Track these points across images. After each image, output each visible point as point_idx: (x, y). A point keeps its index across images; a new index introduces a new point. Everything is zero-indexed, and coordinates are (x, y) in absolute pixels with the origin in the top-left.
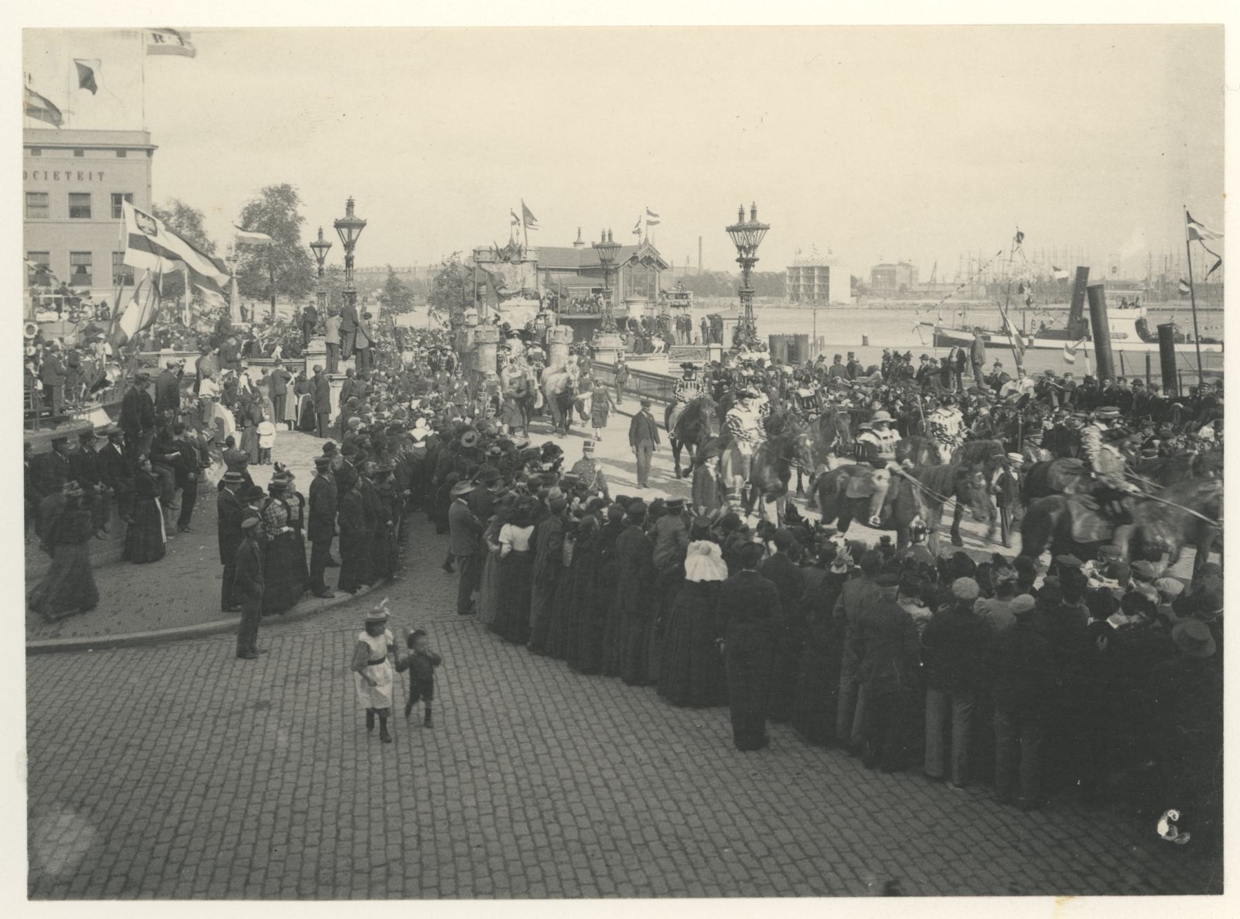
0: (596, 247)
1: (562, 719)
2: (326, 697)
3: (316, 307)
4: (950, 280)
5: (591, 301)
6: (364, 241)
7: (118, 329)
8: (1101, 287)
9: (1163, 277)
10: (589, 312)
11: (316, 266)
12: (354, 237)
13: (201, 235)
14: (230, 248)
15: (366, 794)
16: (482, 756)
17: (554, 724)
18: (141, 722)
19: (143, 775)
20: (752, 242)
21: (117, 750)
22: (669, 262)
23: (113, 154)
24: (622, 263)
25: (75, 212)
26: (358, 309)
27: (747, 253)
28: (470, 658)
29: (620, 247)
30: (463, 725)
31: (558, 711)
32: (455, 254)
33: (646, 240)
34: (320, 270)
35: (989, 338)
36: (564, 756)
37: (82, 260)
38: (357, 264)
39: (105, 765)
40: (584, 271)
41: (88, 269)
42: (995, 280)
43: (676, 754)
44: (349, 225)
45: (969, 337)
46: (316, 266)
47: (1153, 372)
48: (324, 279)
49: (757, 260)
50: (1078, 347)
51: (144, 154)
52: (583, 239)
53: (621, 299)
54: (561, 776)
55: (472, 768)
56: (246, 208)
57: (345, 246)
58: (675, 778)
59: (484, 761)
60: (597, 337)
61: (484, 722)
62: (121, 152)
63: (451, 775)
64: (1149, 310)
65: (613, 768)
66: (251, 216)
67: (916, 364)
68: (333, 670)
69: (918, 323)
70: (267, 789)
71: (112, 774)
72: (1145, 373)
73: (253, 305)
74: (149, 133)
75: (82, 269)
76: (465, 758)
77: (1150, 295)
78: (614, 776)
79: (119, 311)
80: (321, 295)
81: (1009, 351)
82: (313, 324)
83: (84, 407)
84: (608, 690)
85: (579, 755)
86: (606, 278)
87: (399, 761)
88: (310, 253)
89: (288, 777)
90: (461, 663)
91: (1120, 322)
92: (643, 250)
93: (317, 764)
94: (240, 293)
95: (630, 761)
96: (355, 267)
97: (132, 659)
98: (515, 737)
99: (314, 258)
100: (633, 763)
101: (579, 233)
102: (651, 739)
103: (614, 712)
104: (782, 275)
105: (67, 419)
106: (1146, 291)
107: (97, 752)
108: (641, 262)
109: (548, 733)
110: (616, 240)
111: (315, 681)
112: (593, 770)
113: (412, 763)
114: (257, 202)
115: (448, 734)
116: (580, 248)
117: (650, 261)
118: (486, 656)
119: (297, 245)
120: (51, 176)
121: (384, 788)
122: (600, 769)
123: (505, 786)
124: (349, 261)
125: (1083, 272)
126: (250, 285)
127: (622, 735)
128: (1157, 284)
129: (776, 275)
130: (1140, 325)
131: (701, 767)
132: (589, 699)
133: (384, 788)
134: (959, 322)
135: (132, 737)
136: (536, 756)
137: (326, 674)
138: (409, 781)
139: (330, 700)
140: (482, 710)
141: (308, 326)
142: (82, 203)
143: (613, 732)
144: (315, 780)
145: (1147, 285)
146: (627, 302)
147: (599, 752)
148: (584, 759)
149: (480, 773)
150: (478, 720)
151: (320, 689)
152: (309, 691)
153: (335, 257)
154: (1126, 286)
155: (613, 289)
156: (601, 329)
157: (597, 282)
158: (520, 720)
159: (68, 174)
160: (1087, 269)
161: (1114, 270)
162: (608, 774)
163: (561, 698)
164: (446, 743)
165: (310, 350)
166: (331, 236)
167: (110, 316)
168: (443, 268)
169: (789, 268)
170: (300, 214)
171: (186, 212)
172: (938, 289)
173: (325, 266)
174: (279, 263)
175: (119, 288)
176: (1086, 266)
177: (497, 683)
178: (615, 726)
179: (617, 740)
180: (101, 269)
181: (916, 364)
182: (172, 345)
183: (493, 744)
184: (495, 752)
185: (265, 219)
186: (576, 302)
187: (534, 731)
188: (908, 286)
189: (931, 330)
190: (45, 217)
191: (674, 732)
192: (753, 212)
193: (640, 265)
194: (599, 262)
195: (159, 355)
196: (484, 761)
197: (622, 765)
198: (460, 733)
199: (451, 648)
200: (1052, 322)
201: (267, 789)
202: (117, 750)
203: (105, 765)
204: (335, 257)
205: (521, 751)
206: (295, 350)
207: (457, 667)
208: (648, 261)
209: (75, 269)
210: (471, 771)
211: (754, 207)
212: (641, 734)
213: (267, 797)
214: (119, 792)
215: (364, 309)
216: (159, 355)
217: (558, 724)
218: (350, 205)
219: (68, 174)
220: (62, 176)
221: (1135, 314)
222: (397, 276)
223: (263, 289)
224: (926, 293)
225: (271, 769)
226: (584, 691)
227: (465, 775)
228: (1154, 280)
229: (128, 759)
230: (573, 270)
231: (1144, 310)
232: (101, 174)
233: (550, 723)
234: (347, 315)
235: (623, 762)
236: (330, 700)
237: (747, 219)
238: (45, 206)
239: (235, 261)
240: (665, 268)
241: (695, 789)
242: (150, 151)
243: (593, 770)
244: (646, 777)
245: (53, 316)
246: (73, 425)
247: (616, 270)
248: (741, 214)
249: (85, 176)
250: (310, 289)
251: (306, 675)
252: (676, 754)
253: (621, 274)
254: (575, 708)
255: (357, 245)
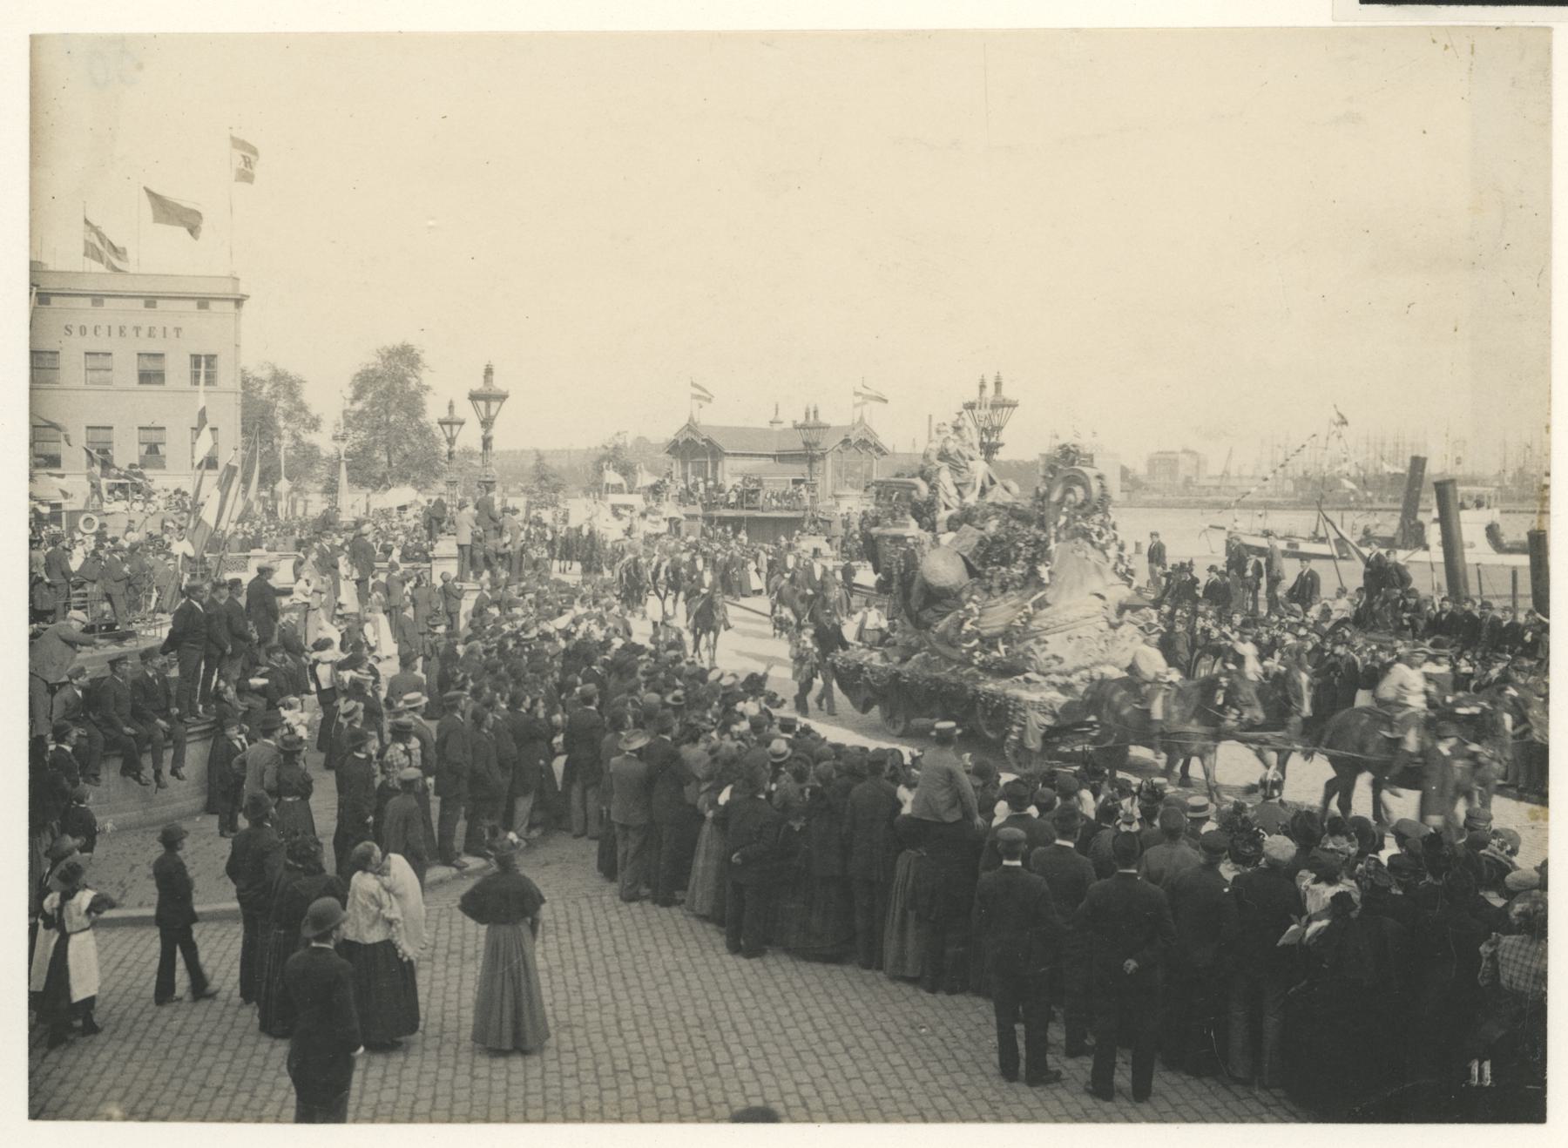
0: (796, 427)
1: (751, 1022)
2: (454, 988)
3: (445, 499)
4: (1248, 471)
5: (792, 495)
6: (505, 417)
7: (199, 522)
8: (1452, 481)
9: (1521, 470)
10: (788, 509)
11: (445, 448)
12: (493, 412)
13: (302, 408)
14: (338, 425)
15: (503, 1110)
16: (648, 1065)
17: (739, 1026)
18: (222, 1016)
19: (224, 1082)
20: (996, 423)
21: (194, 1050)
22: (890, 448)
23: (193, 304)
24: (829, 448)
25: (146, 377)
26: (497, 501)
27: (989, 437)
28: (635, 943)
29: (828, 427)
30: (624, 1025)
31: (744, 1010)
32: (618, 434)
33: (861, 418)
34: (450, 454)
35: (1296, 546)
36: (751, 1067)
37: (153, 436)
38: (497, 445)
39: (177, 1068)
40: (781, 457)
41: (161, 448)
42: (1305, 473)
43: (893, 1067)
44: (489, 398)
45: (1262, 543)
46: (445, 448)
47: (1520, 591)
48: (455, 465)
49: (1002, 445)
50: (1411, 559)
51: (232, 304)
52: (781, 417)
53: (829, 492)
54: (748, 1092)
55: (636, 1079)
56: (358, 374)
57: (482, 423)
58: (892, 1097)
59: (651, 1071)
60: (798, 540)
61: (652, 1023)
62: (203, 302)
63: (611, 1089)
64: (1502, 512)
65: (813, 1084)
66: (364, 381)
67: (1203, 577)
68: (462, 953)
69: (1207, 526)
70: (379, 1102)
71: (186, 1079)
72: (1510, 592)
73: (368, 495)
74: (237, 279)
75: (153, 449)
76: (627, 1067)
77: (1505, 496)
78: (814, 1094)
79: (200, 500)
80: (452, 483)
81: (1331, 562)
82: (440, 521)
83: (154, 620)
84: (807, 986)
85: (770, 1066)
86: (810, 467)
87: (544, 1070)
88: (438, 432)
89: (405, 1087)
90: (622, 948)
91: (1472, 525)
92: (858, 430)
93: (441, 1071)
94: (349, 481)
95: (834, 1075)
96: (494, 449)
97: (211, 937)
98: (690, 1040)
99: (444, 439)
100: (839, 1077)
101: (777, 410)
102: (861, 1047)
103: (816, 1012)
104: (1035, 463)
105: (132, 634)
106: (1499, 488)
107: (167, 1052)
108: (855, 446)
109: (732, 1038)
110: (824, 418)
111: (440, 967)
112: (788, 1086)
113: (560, 1072)
114: (371, 367)
115: (605, 1036)
116: (777, 427)
117: (868, 445)
118: (655, 939)
119: (421, 420)
120: (115, 331)
121: (525, 1102)
122: (797, 1084)
123: (677, 1104)
124: (487, 442)
125: (1418, 463)
126: (364, 473)
127: (823, 1041)
128: (1514, 479)
129: (1026, 463)
130: (1492, 532)
131: (924, 1083)
132: (783, 996)
133: (525, 1102)
134: (1260, 524)
135: (212, 1033)
136: (717, 1065)
137: (455, 959)
138: (556, 1095)
139: (459, 992)
140: (649, 1007)
141: (434, 522)
142: (151, 365)
143: (813, 1037)
144: (439, 1092)
145: (1503, 481)
146: (837, 497)
147: (795, 1063)
148: (777, 1071)
149: (645, 1086)
150: (644, 1020)
151: (446, 978)
152: (432, 979)
153: (469, 437)
154: (1473, 481)
155: (818, 479)
156: (803, 531)
157: (798, 470)
158: (696, 1022)
159: (137, 329)
160: (1425, 460)
161: (1459, 461)
162: (806, 1090)
163: (748, 994)
164: (604, 1048)
165: (436, 552)
166: (465, 410)
167: (186, 505)
168: (603, 452)
169: (1042, 455)
170: (425, 383)
171: (283, 378)
172: (1232, 483)
173: (456, 448)
174: (400, 443)
175: (199, 472)
176: (1422, 455)
177: (668, 974)
178: (816, 1030)
179: (819, 1049)
180: (175, 446)
181: (1203, 577)
182: (265, 546)
183: (662, 1050)
184: (665, 1062)
185: (382, 387)
186: (772, 496)
187: (713, 1035)
188: (1194, 479)
189: (1223, 536)
190: (108, 383)
191: (890, 1039)
192: (998, 385)
193: (853, 450)
194: (802, 446)
195: (248, 557)
196: (651, 1071)
197: (824, 1080)
198: (621, 1035)
199: (611, 929)
200: (1377, 526)
201: (379, 1102)
202: (194, 1050)
203: (177, 1068)
204: (469, 437)
205: (697, 1060)
206: (419, 555)
207: (618, 953)
208: (864, 443)
209: (144, 448)
210: (635, 1084)
211: (998, 377)
212: (848, 1040)
213: (380, 1111)
214: (195, 1102)
215: (504, 501)
216: (248, 557)
217: (745, 1028)
218: (489, 371)
219: (137, 329)
220: (129, 331)
221: (1491, 515)
222: (547, 461)
223: (379, 475)
224: (1218, 488)
225: (385, 1076)
226: (777, 985)
227: (627, 1089)
228: (1510, 474)
229: (207, 1061)
230: (769, 456)
231: (1497, 511)
232: (178, 330)
233: (734, 1025)
234: (484, 507)
235: (826, 1076)
236: (459, 992)
237: (990, 392)
238: (109, 370)
239: (344, 440)
240: (885, 454)
241: (915, 1112)
242: (239, 302)
243: (788, 1086)
244: (854, 1095)
245: (120, 506)
246: (141, 642)
247: (823, 455)
248: (982, 386)
249: (159, 332)
250: (436, 476)
251: (429, 960)
252: (893, 1067)
253: (829, 460)
254: (766, 1007)
255: (496, 421)
